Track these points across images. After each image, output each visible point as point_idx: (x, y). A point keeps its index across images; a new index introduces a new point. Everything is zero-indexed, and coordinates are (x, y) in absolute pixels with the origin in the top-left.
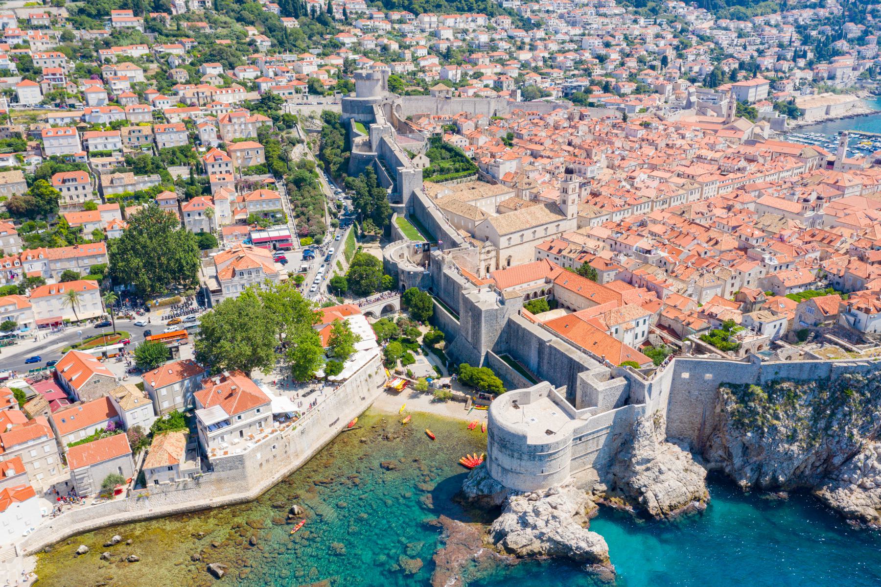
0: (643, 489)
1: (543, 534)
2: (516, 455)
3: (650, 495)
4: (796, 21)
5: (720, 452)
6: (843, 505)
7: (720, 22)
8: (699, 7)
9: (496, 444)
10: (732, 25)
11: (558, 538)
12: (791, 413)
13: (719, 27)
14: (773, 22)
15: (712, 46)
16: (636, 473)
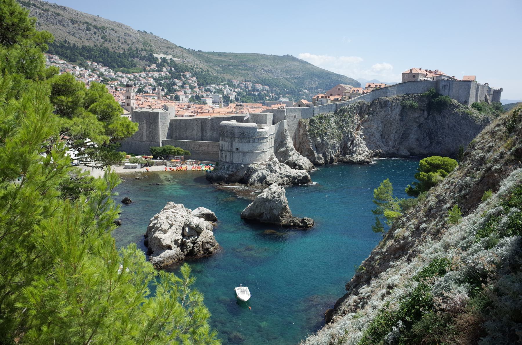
0: (296, 162)
1: (281, 174)
2: (251, 140)
3: (301, 164)
4: (152, 76)
5: (307, 153)
6: (358, 160)
7: (118, 73)
8: (105, 66)
9: (237, 139)
10: (124, 75)
11: (289, 174)
12: (329, 126)
13: (118, 76)
14: (142, 76)
15: (119, 83)
16: (290, 156)
